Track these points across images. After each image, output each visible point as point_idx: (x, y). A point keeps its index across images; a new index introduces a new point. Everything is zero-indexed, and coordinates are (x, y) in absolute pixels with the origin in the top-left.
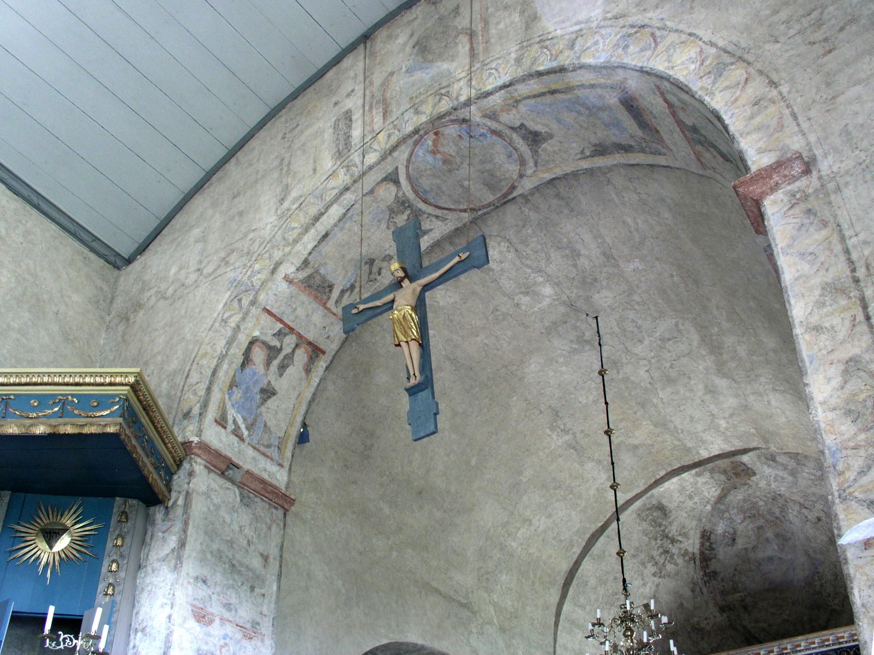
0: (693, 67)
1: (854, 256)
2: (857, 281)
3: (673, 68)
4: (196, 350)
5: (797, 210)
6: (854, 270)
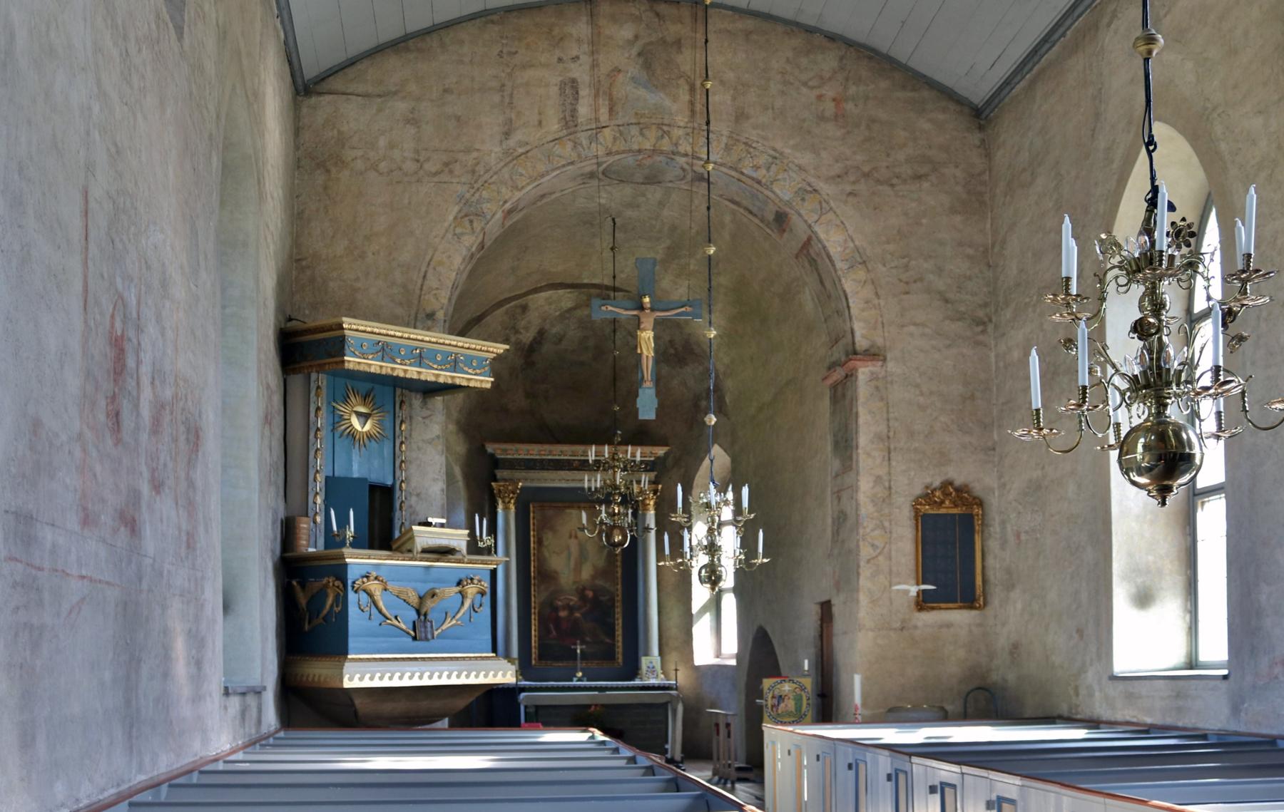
0: (839, 249)
1: (891, 423)
2: (889, 437)
3: (828, 241)
4: (430, 252)
5: (874, 383)
6: (889, 431)
